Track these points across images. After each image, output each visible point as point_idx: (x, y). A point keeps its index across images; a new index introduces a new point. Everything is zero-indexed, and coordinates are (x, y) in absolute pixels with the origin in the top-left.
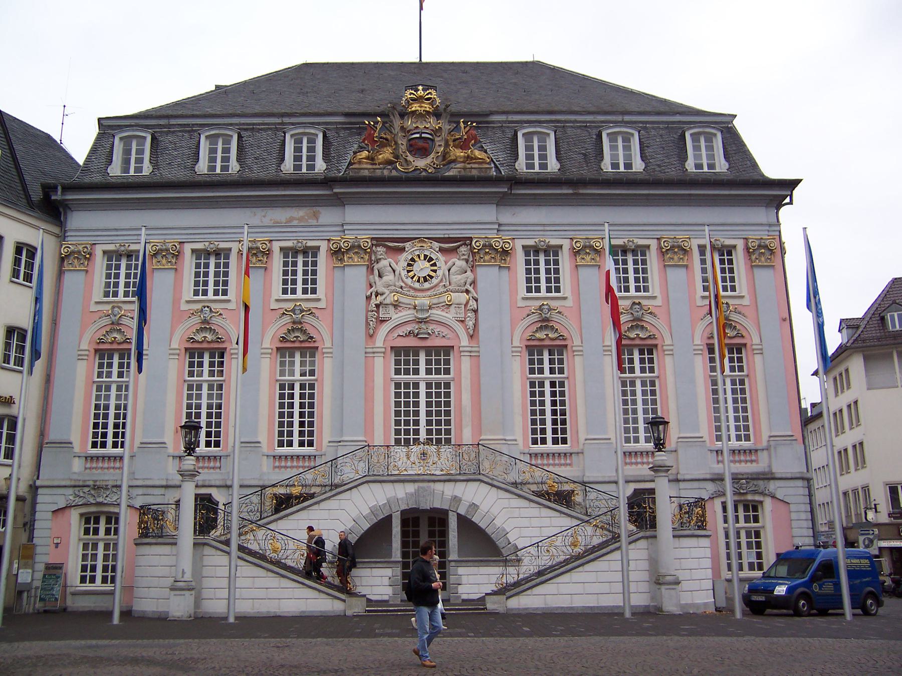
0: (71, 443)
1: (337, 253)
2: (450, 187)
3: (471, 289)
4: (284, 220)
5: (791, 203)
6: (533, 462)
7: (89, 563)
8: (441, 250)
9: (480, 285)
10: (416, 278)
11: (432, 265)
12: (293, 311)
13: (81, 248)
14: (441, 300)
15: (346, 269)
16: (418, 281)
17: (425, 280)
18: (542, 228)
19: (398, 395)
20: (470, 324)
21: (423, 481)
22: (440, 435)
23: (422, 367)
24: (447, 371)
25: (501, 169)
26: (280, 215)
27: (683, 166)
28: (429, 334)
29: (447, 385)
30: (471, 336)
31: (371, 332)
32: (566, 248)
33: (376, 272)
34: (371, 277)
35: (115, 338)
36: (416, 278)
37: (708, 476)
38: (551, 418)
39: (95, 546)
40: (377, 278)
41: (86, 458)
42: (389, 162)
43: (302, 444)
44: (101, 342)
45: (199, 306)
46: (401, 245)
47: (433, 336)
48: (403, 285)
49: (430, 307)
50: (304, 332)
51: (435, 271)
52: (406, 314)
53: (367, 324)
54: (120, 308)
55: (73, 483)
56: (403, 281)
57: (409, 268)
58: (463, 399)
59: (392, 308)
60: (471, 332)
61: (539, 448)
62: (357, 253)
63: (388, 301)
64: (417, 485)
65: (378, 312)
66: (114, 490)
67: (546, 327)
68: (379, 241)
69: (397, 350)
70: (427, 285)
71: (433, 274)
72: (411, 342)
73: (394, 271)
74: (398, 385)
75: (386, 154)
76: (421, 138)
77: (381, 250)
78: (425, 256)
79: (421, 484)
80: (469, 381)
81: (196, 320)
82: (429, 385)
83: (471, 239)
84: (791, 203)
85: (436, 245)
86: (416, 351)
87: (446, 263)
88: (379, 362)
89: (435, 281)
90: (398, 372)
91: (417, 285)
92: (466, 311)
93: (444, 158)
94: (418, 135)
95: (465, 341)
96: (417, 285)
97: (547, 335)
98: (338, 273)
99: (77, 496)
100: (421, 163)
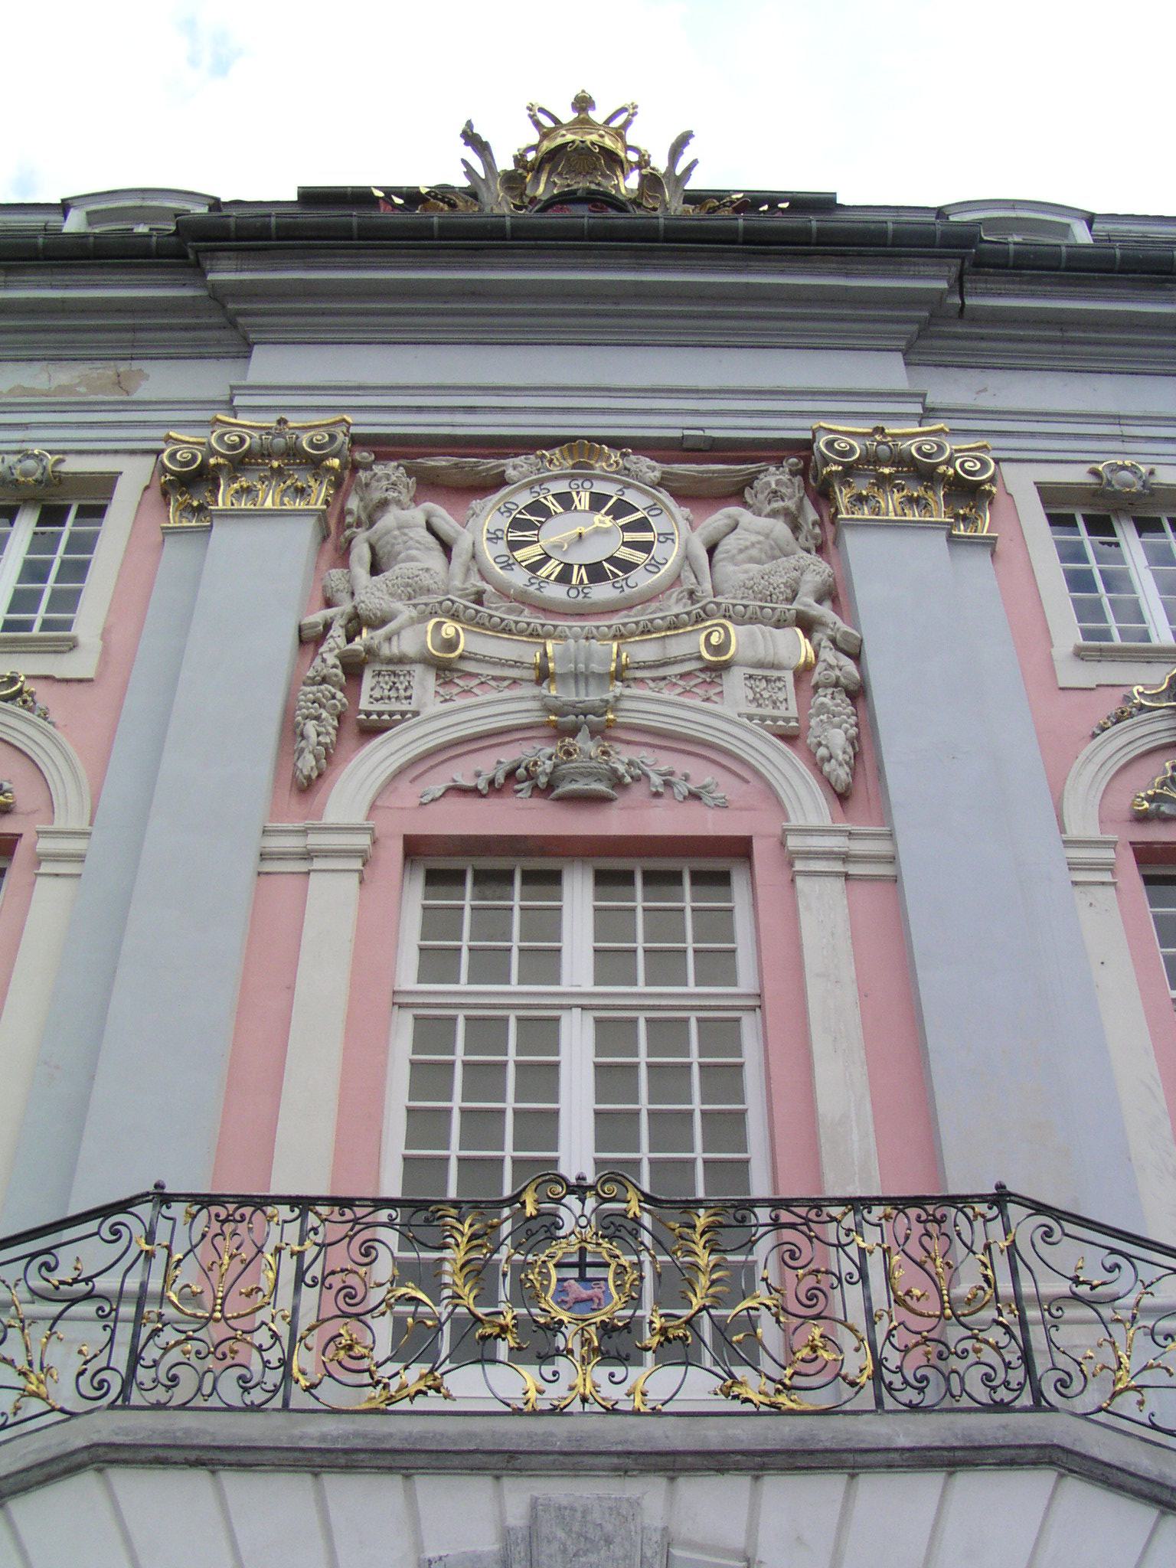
2: (703, 270)
9: (866, 592)
10: (552, 568)
11: (626, 528)
14: (679, 647)
15: (221, 532)
16: (564, 577)
17: (596, 573)
18: (1115, 430)
19: (428, 1077)
20: (837, 739)
21: (574, 1460)
28: (617, 782)
30: (842, 797)
33: (361, 553)
34: (337, 573)
36: (552, 568)
47: (638, 792)
51: (646, 547)
53: (291, 731)
57: (516, 536)
60: (842, 774)
62: (278, 473)
63: (407, 644)
64: (518, 1497)
69: (437, 861)
70: (602, 592)
72: (522, 817)
74: (432, 1030)
77: (390, 471)
78: (598, 502)
79: (559, 1490)
80: (849, 993)
85: (647, 467)
86: (539, 865)
88: (332, 901)
89: (641, 580)
91: (556, 592)
95: (808, 805)
98: (176, 553)
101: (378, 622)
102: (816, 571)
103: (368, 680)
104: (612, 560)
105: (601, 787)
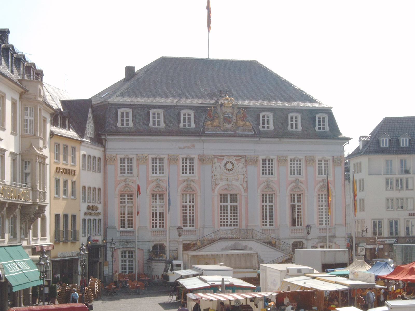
0: (115, 227)
1: (202, 160)
3: (245, 174)
4: (183, 147)
5: (348, 144)
6: (263, 232)
7: (124, 267)
8: (236, 160)
12: (187, 181)
13: (113, 156)
17: (231, 170)
20: (245, 186)
22: (235, 223)
23: (229, 200)
24: (236, 202)
25: (254, 128)
26: (182, 145)
27: (314, 129)
29: (237, 206)
31: (213, 188)
32: (276, 159)
35: (127, 190)
37: (317, 237)
38: (269, 217)
39: (125, 261)
40: (215, 170)
41: (120, 232)
42: (217, 126)
43: (190, 226)
44: (122, 191)
45: (155, 178)
46: (223, 158)
48: (223, 172)
49: (232, 180)
50: (191, 188)
52: (224, 183)
53: (212, 186)
54: (128, 179)
55: (119, 241)
56: (223, 171)
58: (242, 212)
59: (220, 180)
61: (265, 227)
65: (215, 181)
66: (132, 243)
67: (268, 187)
68: (215, 156)
70: (231, 172)
71: (233, 168)
73: (220, 167)
74: (221, 206)
75: (216, 123)
76: (228, 117)
77: (216, 159)
81: (154, 184)
82: (231, 206)
83: (246, 156)
84: (348, 144)
85: (234, 158)
87: (237, 164)
90: (221, 202)
92: (244, 181)
93: (236, 125)
94: (227, 116)
96: (228, 172)
97: (269, 190)
99: (120, 245)
100: (229, 126)
101: (216, 175)
102: (245, 169)
103: (216, 180)
104: (232, 169)
105: (231, 190)
